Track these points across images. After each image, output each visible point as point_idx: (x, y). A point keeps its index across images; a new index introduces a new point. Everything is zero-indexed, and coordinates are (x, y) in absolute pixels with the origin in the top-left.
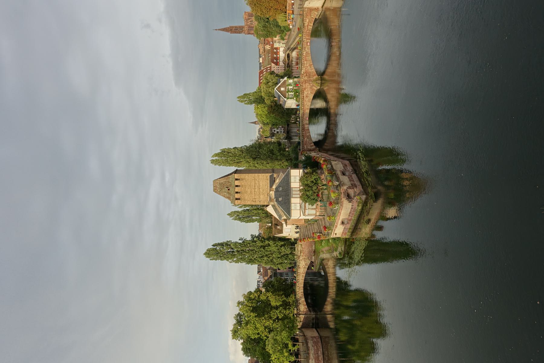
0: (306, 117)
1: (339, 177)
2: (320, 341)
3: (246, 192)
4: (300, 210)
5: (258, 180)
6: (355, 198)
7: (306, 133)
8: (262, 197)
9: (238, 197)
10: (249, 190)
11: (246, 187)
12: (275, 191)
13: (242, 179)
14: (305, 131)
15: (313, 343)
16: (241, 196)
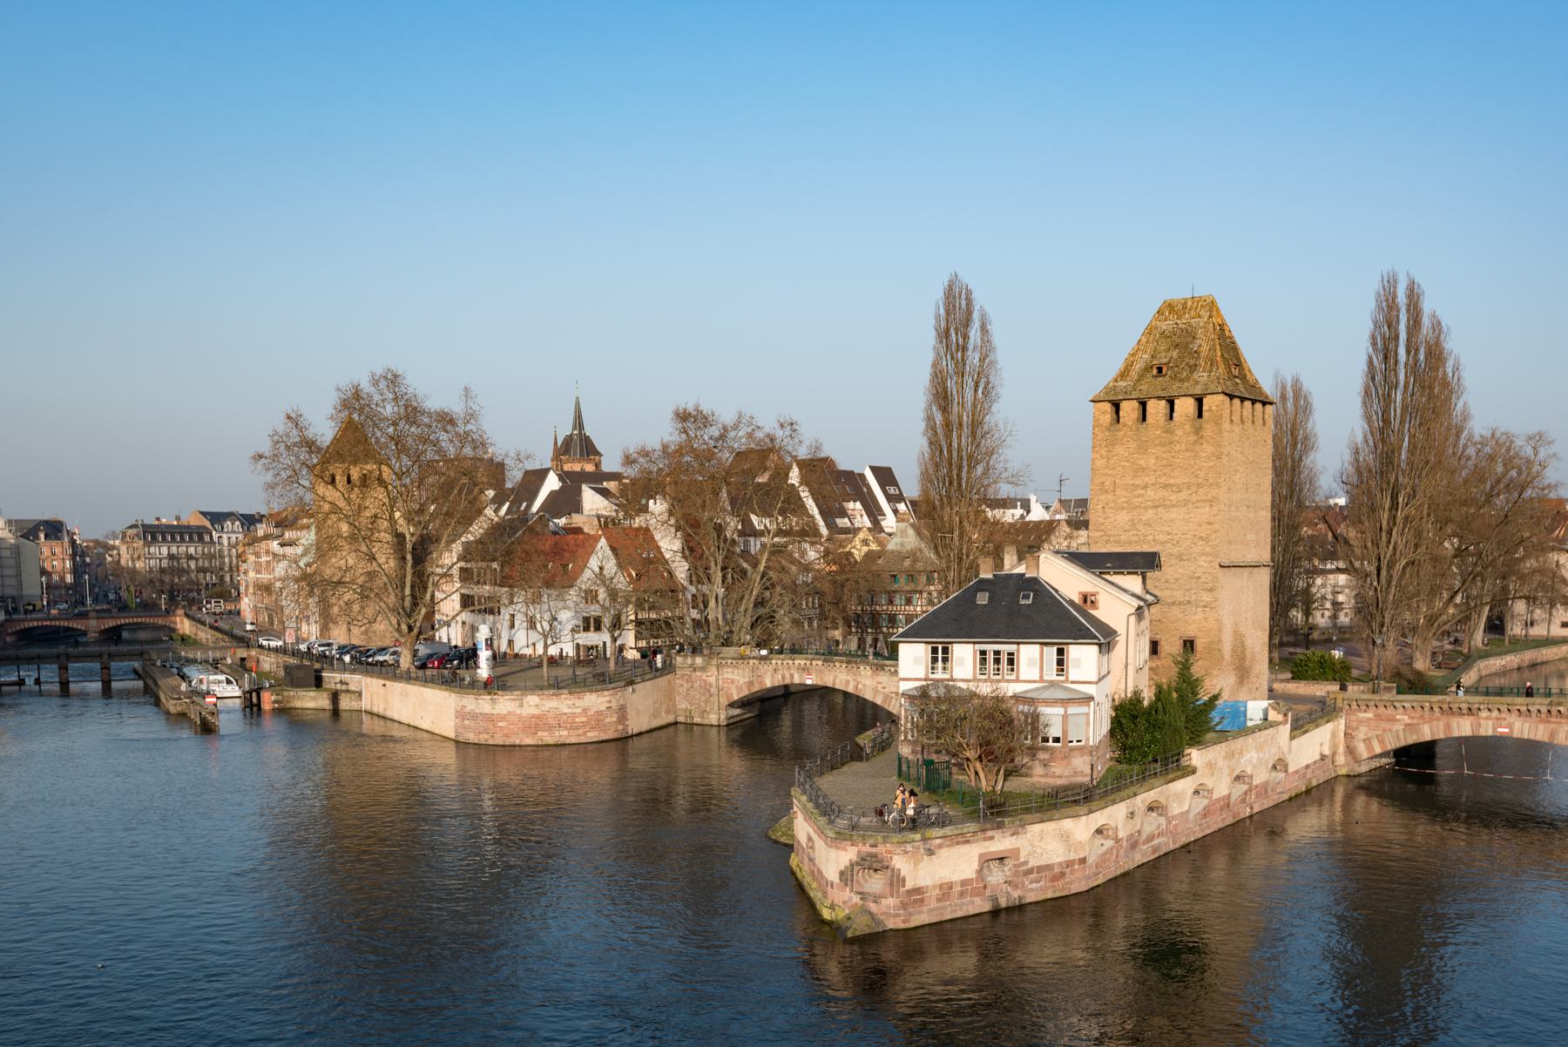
0: (1510, 726)
1: (967, 842)
2: (604, 737)
3: (1142, 448)
4: (925, 680)
5: (1194, 498)
6: (856, 899)
7: (1435, 723)
8: (1123, 518)
9: (1121, 413)
10: (1154, 461)
11: (1164, 446)
12: (1027, 576)
13: (1197, 431)
14: (1444, 719)
15: (599, 713)
16: (1125, 425)
